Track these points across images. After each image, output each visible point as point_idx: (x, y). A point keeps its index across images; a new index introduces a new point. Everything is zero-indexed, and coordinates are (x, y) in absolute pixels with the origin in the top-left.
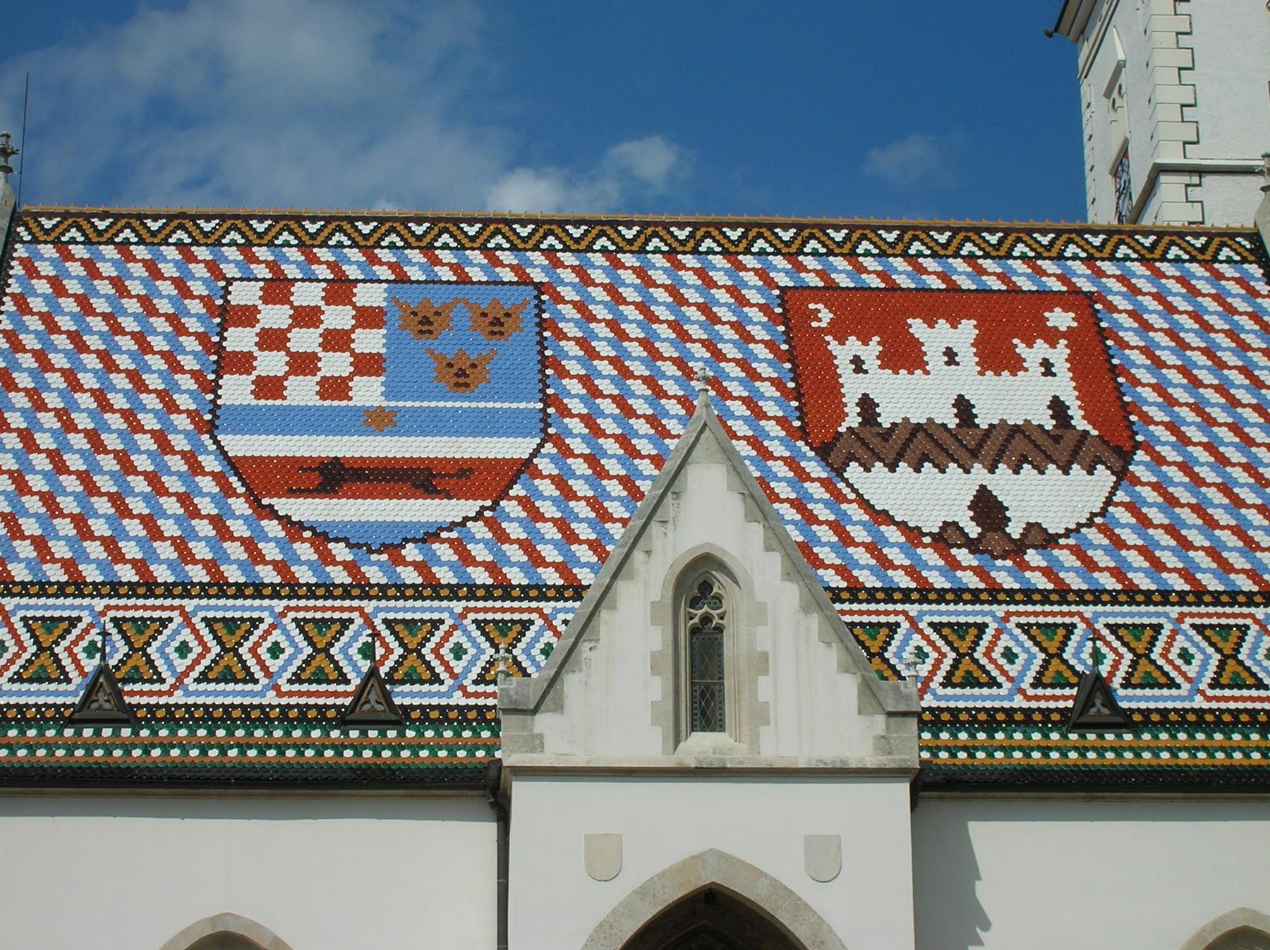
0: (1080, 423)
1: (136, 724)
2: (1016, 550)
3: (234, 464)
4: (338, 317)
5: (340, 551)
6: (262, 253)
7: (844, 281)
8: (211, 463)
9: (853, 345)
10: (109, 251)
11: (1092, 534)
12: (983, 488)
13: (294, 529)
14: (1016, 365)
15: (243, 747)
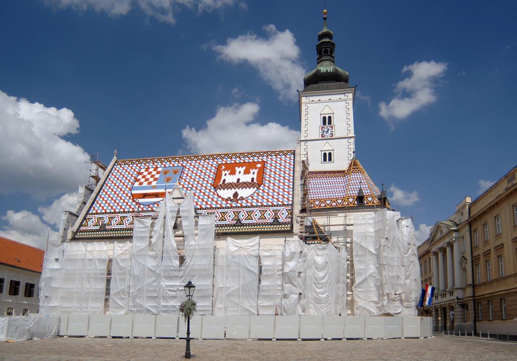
0: (255, 181)
1: (108, 231)
2: (237, 201)
3: (132, 195)
4: (154, 173)
5: (142, 206)
6: (147, 164)
7: (228, 162)
8: (129, 195)
9: (226, 172)
10: (127, 166)
11: (250, 198)
12: (236, 192)
13: (137, 203)
14: (249, 173)
15: (118, 234)
